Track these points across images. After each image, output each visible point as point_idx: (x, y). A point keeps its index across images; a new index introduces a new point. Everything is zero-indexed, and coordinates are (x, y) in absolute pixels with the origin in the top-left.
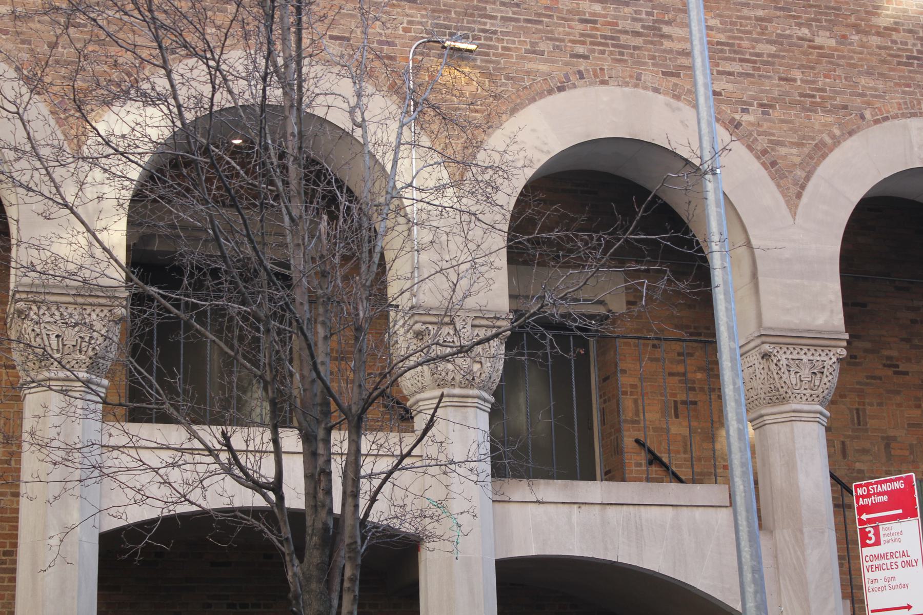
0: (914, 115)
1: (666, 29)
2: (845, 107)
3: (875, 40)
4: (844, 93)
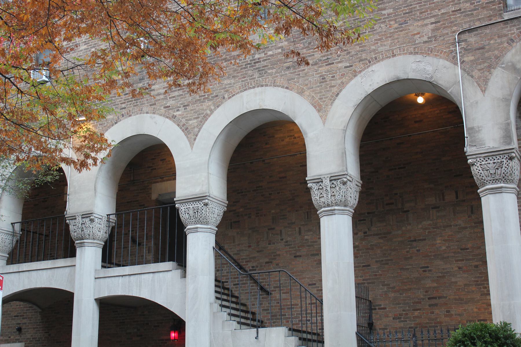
0: (246, 90)
2: (217, 96)
4: (217, 90)
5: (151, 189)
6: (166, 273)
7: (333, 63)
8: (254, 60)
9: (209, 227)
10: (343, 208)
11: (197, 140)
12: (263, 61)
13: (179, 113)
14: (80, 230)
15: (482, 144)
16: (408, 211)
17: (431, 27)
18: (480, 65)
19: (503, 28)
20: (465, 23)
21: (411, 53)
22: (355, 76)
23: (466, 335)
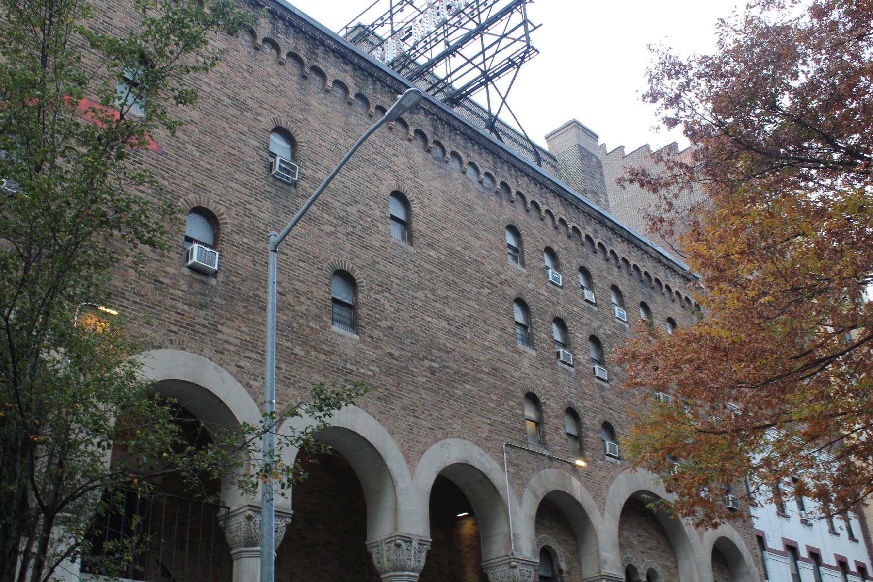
1: (220, 327)
2: (305, 388)
3: (323, 357)
13: (257, 384)
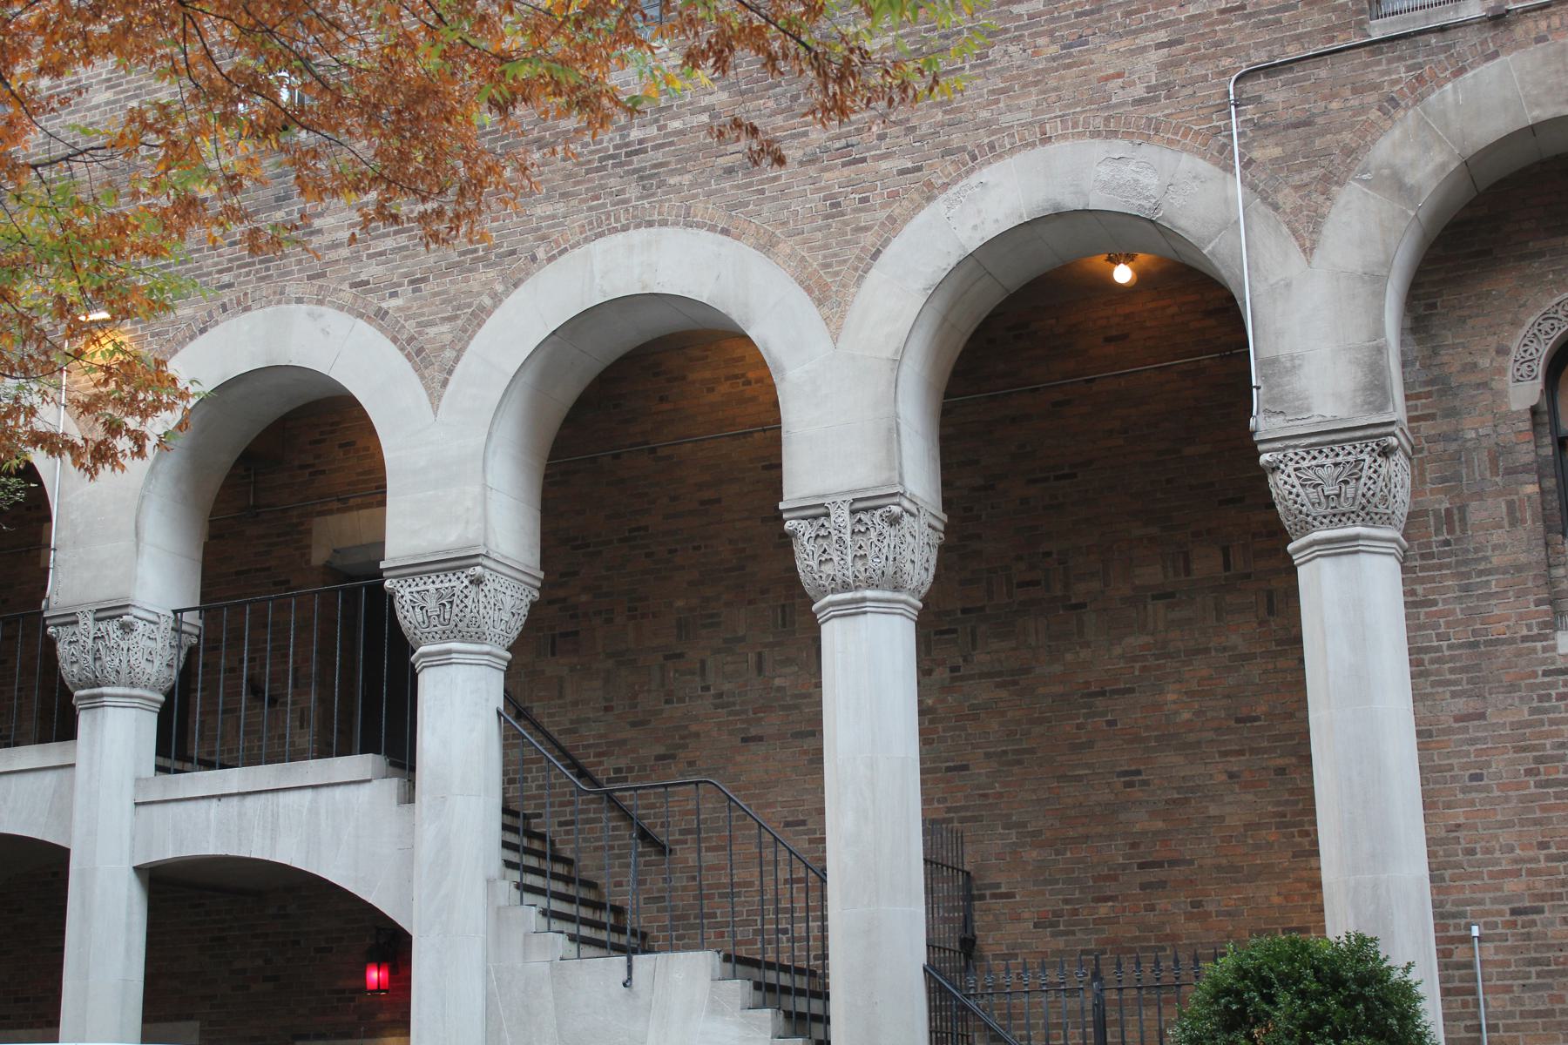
0: (601, 235)
2: (513, 252)
4: (513, 234)
5: (309, 532)
6: (352, 787)
7: (864, 160)
8: (627, 145)
9: (486, 648)
10: (888, 595)
11: (450, 387)
12: (655, 148)
14: (90, 658)
15: (1300, 410)
16: (1083, 605)
17: (1156, 56)
18: (1301, 172)
19: (1367, 65)
20: (1257, 46)
21: (1096, 134)
22: (930, 199)
23: (1246, 972)
